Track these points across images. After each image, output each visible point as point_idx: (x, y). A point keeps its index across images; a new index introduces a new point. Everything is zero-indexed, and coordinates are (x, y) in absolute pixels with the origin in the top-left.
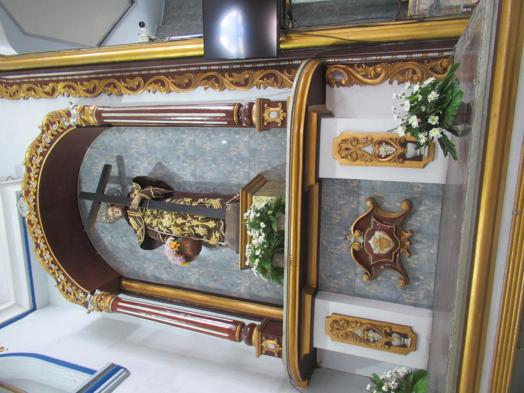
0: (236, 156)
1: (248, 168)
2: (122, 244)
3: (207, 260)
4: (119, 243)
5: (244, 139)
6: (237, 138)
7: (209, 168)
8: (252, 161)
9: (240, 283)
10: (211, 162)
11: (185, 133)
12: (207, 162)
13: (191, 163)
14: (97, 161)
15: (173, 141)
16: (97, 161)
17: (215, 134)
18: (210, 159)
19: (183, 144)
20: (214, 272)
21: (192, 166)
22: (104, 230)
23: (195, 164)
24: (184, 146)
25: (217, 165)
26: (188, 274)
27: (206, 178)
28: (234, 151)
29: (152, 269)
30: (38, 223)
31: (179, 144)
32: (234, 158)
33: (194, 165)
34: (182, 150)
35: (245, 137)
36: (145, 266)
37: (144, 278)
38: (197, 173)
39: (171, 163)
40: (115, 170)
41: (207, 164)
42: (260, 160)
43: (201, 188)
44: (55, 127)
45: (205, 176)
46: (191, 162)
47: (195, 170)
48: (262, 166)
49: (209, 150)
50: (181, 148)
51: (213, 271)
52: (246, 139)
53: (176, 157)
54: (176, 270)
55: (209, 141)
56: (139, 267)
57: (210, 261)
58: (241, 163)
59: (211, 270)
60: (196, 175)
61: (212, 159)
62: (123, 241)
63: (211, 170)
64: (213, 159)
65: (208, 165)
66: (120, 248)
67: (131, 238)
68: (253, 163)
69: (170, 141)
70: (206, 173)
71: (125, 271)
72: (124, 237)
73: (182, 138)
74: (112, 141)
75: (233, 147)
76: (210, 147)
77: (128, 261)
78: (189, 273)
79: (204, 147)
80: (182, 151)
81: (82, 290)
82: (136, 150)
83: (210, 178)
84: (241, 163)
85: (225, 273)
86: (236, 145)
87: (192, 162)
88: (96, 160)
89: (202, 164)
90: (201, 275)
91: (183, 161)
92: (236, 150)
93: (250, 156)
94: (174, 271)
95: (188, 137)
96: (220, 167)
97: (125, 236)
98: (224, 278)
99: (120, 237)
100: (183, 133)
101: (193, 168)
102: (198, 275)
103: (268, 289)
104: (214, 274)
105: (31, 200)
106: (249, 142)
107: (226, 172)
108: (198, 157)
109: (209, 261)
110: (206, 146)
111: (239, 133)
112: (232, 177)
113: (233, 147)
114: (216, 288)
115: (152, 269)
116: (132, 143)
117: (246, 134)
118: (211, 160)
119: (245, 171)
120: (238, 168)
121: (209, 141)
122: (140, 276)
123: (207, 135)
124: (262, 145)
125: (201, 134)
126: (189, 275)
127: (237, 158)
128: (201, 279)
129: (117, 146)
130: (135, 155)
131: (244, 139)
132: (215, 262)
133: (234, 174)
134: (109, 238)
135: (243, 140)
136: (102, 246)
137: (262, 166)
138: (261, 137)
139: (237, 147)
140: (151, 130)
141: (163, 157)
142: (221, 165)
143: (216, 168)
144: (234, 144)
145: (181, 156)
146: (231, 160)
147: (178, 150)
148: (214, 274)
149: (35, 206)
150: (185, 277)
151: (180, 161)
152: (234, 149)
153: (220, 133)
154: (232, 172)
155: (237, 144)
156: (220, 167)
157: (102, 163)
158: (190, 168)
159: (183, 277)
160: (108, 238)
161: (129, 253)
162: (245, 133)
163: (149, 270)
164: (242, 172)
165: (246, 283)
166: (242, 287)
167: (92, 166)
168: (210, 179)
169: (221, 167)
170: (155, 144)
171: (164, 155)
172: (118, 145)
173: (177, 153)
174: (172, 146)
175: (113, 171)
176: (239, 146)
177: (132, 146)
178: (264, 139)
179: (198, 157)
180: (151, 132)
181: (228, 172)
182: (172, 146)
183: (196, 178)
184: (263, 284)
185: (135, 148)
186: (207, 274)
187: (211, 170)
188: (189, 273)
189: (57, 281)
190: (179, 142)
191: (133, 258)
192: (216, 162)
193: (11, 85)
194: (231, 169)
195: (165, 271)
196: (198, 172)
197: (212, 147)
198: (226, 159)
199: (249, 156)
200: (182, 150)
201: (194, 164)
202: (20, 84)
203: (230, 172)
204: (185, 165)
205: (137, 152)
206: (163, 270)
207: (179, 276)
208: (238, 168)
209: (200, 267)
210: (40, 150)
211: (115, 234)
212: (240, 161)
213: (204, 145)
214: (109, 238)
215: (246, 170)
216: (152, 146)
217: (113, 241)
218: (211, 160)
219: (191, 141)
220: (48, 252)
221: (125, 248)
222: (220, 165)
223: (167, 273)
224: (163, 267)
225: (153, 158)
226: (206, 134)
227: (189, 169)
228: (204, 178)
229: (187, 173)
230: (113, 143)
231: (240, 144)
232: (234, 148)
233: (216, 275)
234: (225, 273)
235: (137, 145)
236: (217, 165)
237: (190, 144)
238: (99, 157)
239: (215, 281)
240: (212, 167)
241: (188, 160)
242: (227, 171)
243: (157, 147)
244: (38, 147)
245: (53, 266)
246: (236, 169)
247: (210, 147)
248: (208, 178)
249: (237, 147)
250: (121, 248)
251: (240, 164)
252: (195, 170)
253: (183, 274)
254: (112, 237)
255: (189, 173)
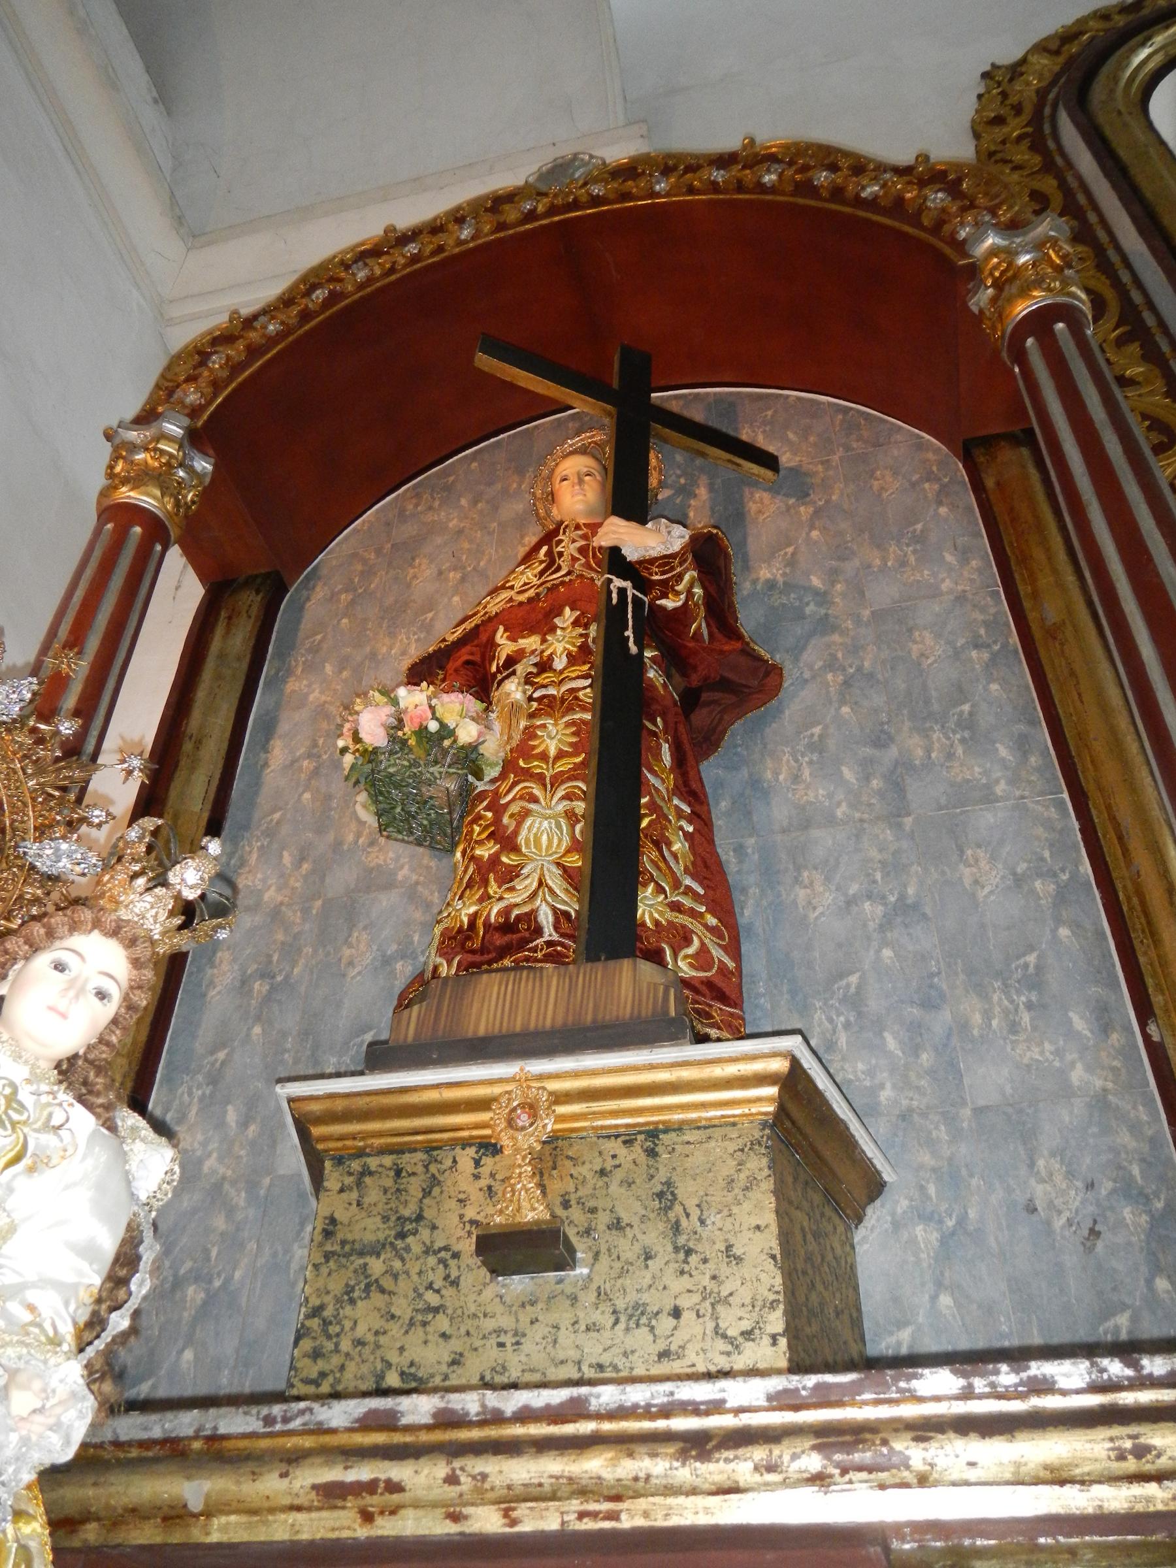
0: (964, 1026)
1: (905, 1102)
2: (428, 572)
3: (356, 934)
4: (431, 562)
5: (1079, 1066)
6: (1070, 1021)
7: (854, 889)
8: (950, 1120)
9: (221, 1124)
10: (892, 899)
11: (1025, 754)
12: (886, 875)
13: (864, 798)
14: (791, 435)
15: (966, 708)
16: (791, 435)
17: (1061, 898)
18: (911, 891)
19: (960, 751)
20: (287, 977)
21: (851, 806)
22: (488, 502)
23: (862, 821)
24: (950, 756)
25: (882, 928)
26: (285, 854)
27: (797, 880)
28: (987, 1015)
29: (311, 698)
30: (501, 226)
31: (954, 732)
32: (946, 1015)
33: (857, 815)
34: (928, 751)
35: (1089, 1069)
36: (328, 669)
37: (273, 672)
38: (815, 833)
39: (845, 710)
40: (762, 503)
41: (878, 876)
42: (971, 1175)
43: (741, 862)
44: (937, 198)
45: (806, 874)
46: (873, 801)
47: (831, 820)
48: (932, 1190)
49: (960, 878)
50: (936, 745)
51: (296, 971)
52: (1077, 1075)
53: (882, 731)
54: (307, 796)
55: (1015, 874)
56: (325, 646)
57: (347, 952)
58: (925, 1058)
59: (302, 961)
60: (806, 825)
61: (909, 901)
62: (440, 573)
63: (851, 902)
64: (915, 907)
65: (875, 882)
66: (412, 566)
67: (456, 599)
68: (942, 1133)
69: (960, 693)
70: (828, 879)
71: (308, 599)
72: (459, 575)
73: (994, 742)
74: (895, 473)
75: (1012, 1002)
76: (976, 882)
77: (353, 603)
78: (287, 858)
79: (969, 852)
80: (920, 752)
81: (209, 403)
82: (878, 562)
83: (801, 902)
84: (924, 1056)
85: (284, 1034)
86: (1026, 1018)
87: (870, 805)
88: (795, 433)
89: (874, 853)
90: (276, 914)
91: (866, 769)
92: (995, 1023)
93: (978, 1111)
94: (301, 790)
95: (1006, 768)
96: (875, 944)
97: (463, 579)
98: (257, 1030)
99: (460, 560)
100: (1022, 745)
101: (839, 813)
102: (280, 898)
103: (178, 1295)
104: (279, 978)
105: (596, 190)
106: (1066, 1092)
107: (854, 979)
108: (907, 828)
109: (350, 946)
110: (977, 861)
111: (1105, 1029)
112: (831, 1020)
113: (1012, 1002)
114: (204, 995)
115: (315, 696)
116: (908, 545)
117: (1113, 1069)
118: (902, 897)
119: (882, 1086)
120: (891, 1043)
121: (1015, 874)
122: (281, 655)
123: (1042, 859)
124: (1070, 1174)
125: (1040, 831)
126: (281, 857)
127: (949, 1036)
128: (258, 919)
129: (880, 495)
130: (850, 567)
131: (1079, 1066)
132: (344, 975)
133: (847, 1026)
134: (451, 525)
135: (1069, 1057)
136: (417, 505)
137: (932, 1190)
138: (1120, 1167)
139: (1014, 1027)
140: (992, 610)
141: (871, 676)
142: (887, 953)
143: (865, 925)
144: (1029, 1006)
145: (894, 751)
146: (929, 1004)
147: (925, 734)
148: (279, 978)
149: (576, 205)
150: (270, 843)
151: (868, 751)
152: (997, 1010)
153: (1076, 926)
154: (860, 1014)
155: (1035, 1028)
156: (875, 944)
157: (788, 455)
158: (840, 796)
159: (270, 833)
160: (455, 522)
161: (389, 601)
162: (1115, 1063)
163: (309, 686)
164: (871, 1073)
165: (220, 1159)
166: (200, 1137)
167: (764, 423)
168: (795, 902)
169: (878, 951)
170: (927, 634)
171: (880, 676)
172: (885, 495)
173: (905, 729)
174: (936, 707)
175: (757, 495)
176: (1022, 1037)
177: (893, 548)
178: (1110, 1185)
179: (907, 828)
180: (983, 610)
181: (853, 990)
182: (936, 707)
183: (783, 831)
184: (208, 1259)
185: (884, 560)
186: (283, 943)
187: (851, 902)
188: (287, 858)
189: (255, 317)
190: (967, 734)
191: (365, 620)
192: (899, 920)
193: (1037, 143)
194: (874, 1004)
195: (302, 750)
196: (823, 840)
197: (981, 894)
198: (932, 975)
199: (981, 1103)
200: (928, 751)
201: (866, 816)
202: (1049, 167)
203: (855, 1001)
204: (848, 774)
205: (869, 566)
206: (308, 743)
207: (277, 816)
208: (891, 1043)
209: (319, 903)
210: (822, 177)
211: (471, 541)
212: (936, 1050)
213: (980, 853)
214: (451, 525)
215: (886, 1095)
216: (911, 623)
217: (439, 540)
218: (902, 897)
219: (988, 787)
220: (378, 271)
221: (409, 586)
222: (885, 943)
223: (293, 762)
224: (321, 741)
225: (852, 633)
226: (1047, 854)
227: (830, 796)
228: (798, 869)
229: (808, 787)
230: (889, 479)
231: (1040, 1044)
232: (1006, 1012)
233: (270, 992)
234: (284, 1034)
235: (903, 563)
236: (881, 926)
237: (968, 781)
238: (812, 439)
239: (245, 982)
240: (867, 905)
241: (876, 783)
242: (859, 987)
243: (915, 642)
244: (834, 168)
245: (320, 295)
246: (880, 1034)
247: (976, 882)
248: (802, 894)
249: (1014, 1027)
250: (412, 571)
251: (917, 1056)
252: (831, 820)
253: (285, 830)
254: (460, 532)
255: (811, 797)
